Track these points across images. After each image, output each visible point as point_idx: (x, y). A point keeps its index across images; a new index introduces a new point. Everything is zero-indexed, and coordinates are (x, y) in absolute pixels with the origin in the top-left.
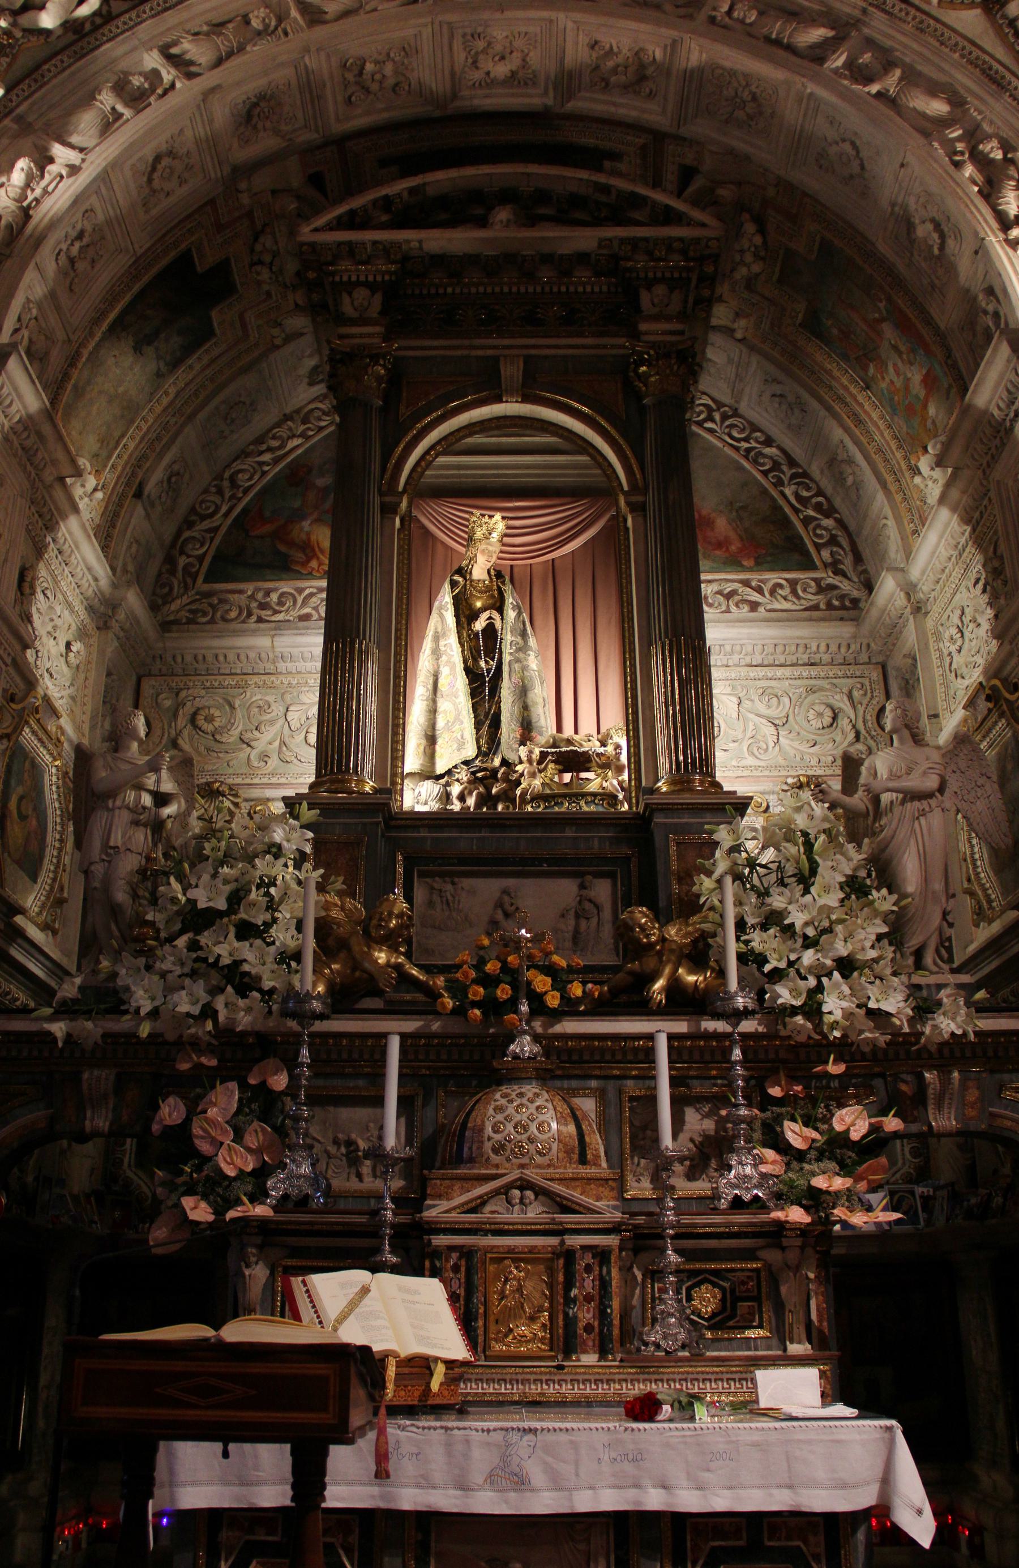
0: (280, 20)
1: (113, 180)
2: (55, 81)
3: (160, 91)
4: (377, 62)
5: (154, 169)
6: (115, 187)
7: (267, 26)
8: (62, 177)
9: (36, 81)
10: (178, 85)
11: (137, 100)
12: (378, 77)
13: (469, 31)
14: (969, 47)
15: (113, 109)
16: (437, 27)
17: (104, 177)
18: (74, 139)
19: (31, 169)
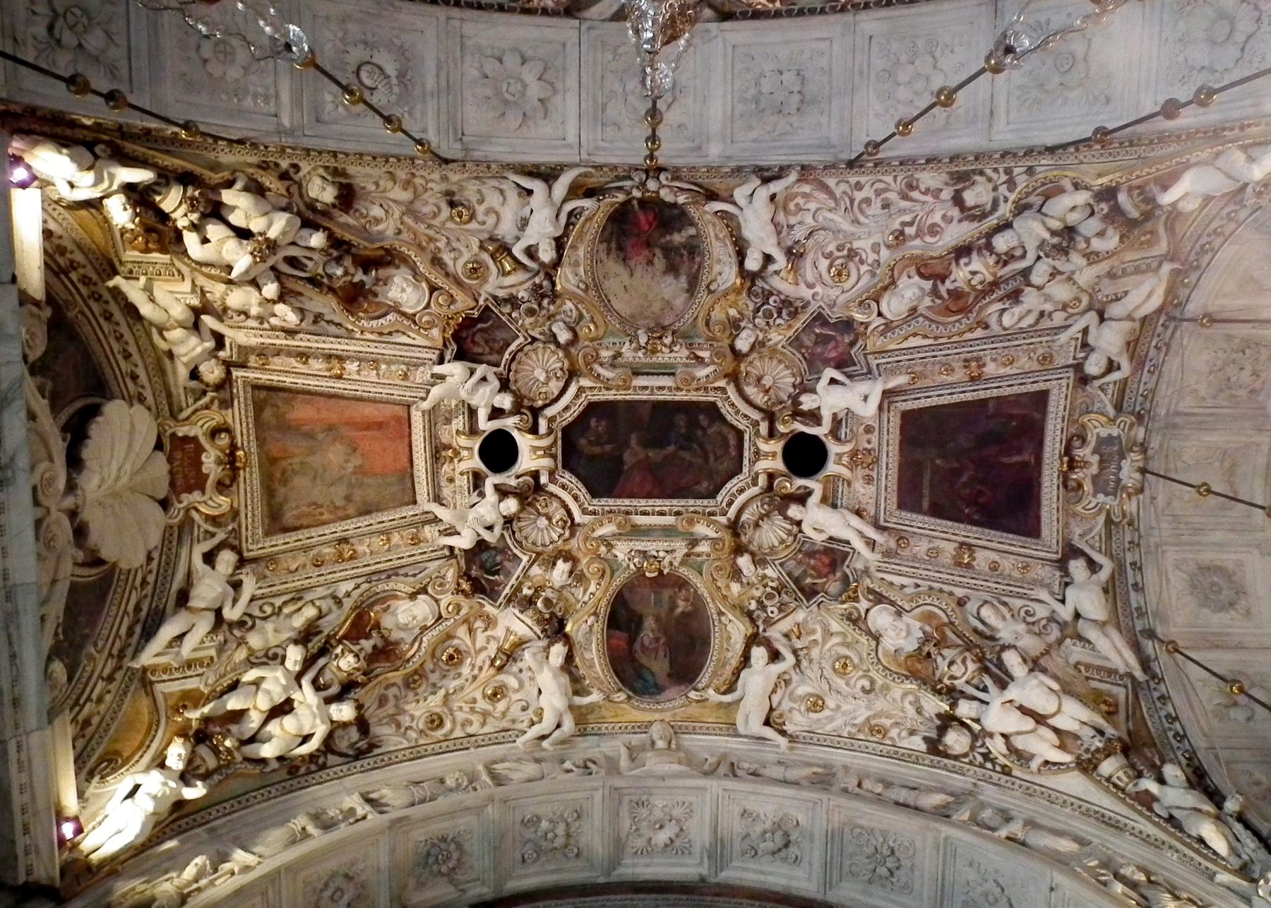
0: (471, 782)
1: (283, 885)
2: (257, 807)
3: (351, 820)
4: (551, 821)
5: (326, 885)
6: (284, 892)
7: (459, 786)
8: (233, 874)
9: (239, 802)
10: (369, 817)
11: (327, 825)
12: (550, 835)
13: (635, 798)
14: (1078, 802)
15: (304, 829)
16: (607, 792)
17: (273, 877)
18: (256, 849)
19: (205, 865)
